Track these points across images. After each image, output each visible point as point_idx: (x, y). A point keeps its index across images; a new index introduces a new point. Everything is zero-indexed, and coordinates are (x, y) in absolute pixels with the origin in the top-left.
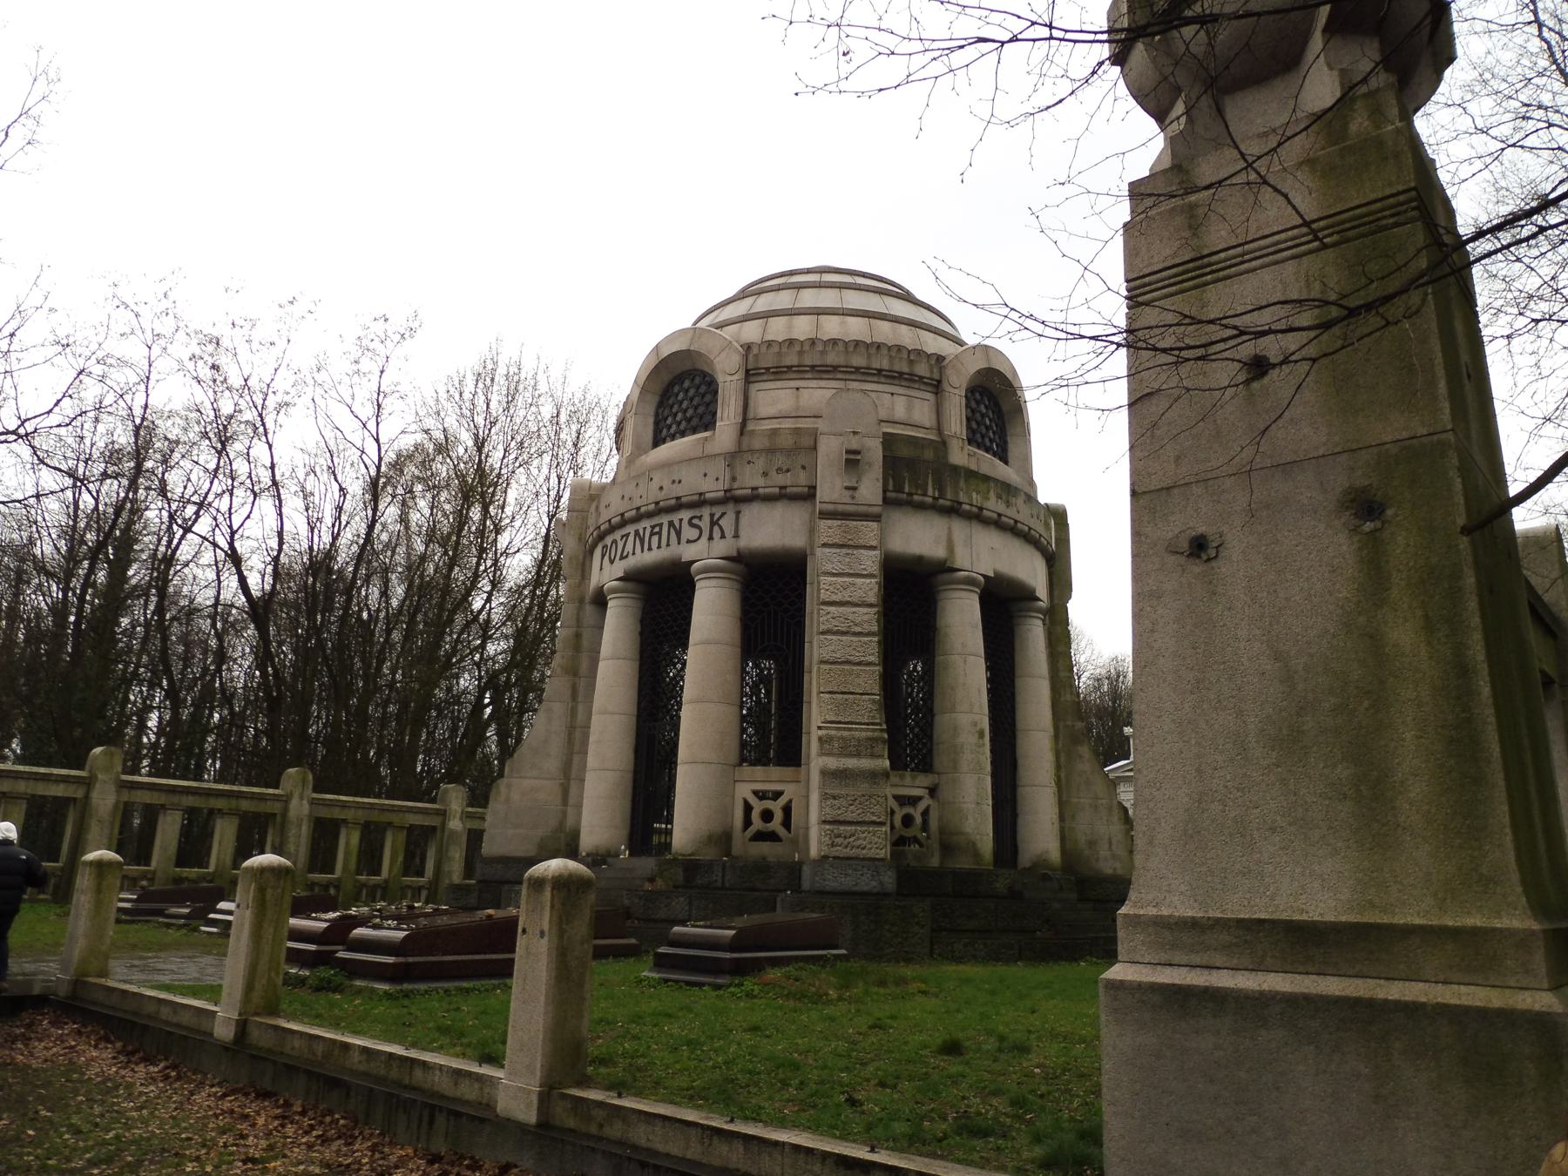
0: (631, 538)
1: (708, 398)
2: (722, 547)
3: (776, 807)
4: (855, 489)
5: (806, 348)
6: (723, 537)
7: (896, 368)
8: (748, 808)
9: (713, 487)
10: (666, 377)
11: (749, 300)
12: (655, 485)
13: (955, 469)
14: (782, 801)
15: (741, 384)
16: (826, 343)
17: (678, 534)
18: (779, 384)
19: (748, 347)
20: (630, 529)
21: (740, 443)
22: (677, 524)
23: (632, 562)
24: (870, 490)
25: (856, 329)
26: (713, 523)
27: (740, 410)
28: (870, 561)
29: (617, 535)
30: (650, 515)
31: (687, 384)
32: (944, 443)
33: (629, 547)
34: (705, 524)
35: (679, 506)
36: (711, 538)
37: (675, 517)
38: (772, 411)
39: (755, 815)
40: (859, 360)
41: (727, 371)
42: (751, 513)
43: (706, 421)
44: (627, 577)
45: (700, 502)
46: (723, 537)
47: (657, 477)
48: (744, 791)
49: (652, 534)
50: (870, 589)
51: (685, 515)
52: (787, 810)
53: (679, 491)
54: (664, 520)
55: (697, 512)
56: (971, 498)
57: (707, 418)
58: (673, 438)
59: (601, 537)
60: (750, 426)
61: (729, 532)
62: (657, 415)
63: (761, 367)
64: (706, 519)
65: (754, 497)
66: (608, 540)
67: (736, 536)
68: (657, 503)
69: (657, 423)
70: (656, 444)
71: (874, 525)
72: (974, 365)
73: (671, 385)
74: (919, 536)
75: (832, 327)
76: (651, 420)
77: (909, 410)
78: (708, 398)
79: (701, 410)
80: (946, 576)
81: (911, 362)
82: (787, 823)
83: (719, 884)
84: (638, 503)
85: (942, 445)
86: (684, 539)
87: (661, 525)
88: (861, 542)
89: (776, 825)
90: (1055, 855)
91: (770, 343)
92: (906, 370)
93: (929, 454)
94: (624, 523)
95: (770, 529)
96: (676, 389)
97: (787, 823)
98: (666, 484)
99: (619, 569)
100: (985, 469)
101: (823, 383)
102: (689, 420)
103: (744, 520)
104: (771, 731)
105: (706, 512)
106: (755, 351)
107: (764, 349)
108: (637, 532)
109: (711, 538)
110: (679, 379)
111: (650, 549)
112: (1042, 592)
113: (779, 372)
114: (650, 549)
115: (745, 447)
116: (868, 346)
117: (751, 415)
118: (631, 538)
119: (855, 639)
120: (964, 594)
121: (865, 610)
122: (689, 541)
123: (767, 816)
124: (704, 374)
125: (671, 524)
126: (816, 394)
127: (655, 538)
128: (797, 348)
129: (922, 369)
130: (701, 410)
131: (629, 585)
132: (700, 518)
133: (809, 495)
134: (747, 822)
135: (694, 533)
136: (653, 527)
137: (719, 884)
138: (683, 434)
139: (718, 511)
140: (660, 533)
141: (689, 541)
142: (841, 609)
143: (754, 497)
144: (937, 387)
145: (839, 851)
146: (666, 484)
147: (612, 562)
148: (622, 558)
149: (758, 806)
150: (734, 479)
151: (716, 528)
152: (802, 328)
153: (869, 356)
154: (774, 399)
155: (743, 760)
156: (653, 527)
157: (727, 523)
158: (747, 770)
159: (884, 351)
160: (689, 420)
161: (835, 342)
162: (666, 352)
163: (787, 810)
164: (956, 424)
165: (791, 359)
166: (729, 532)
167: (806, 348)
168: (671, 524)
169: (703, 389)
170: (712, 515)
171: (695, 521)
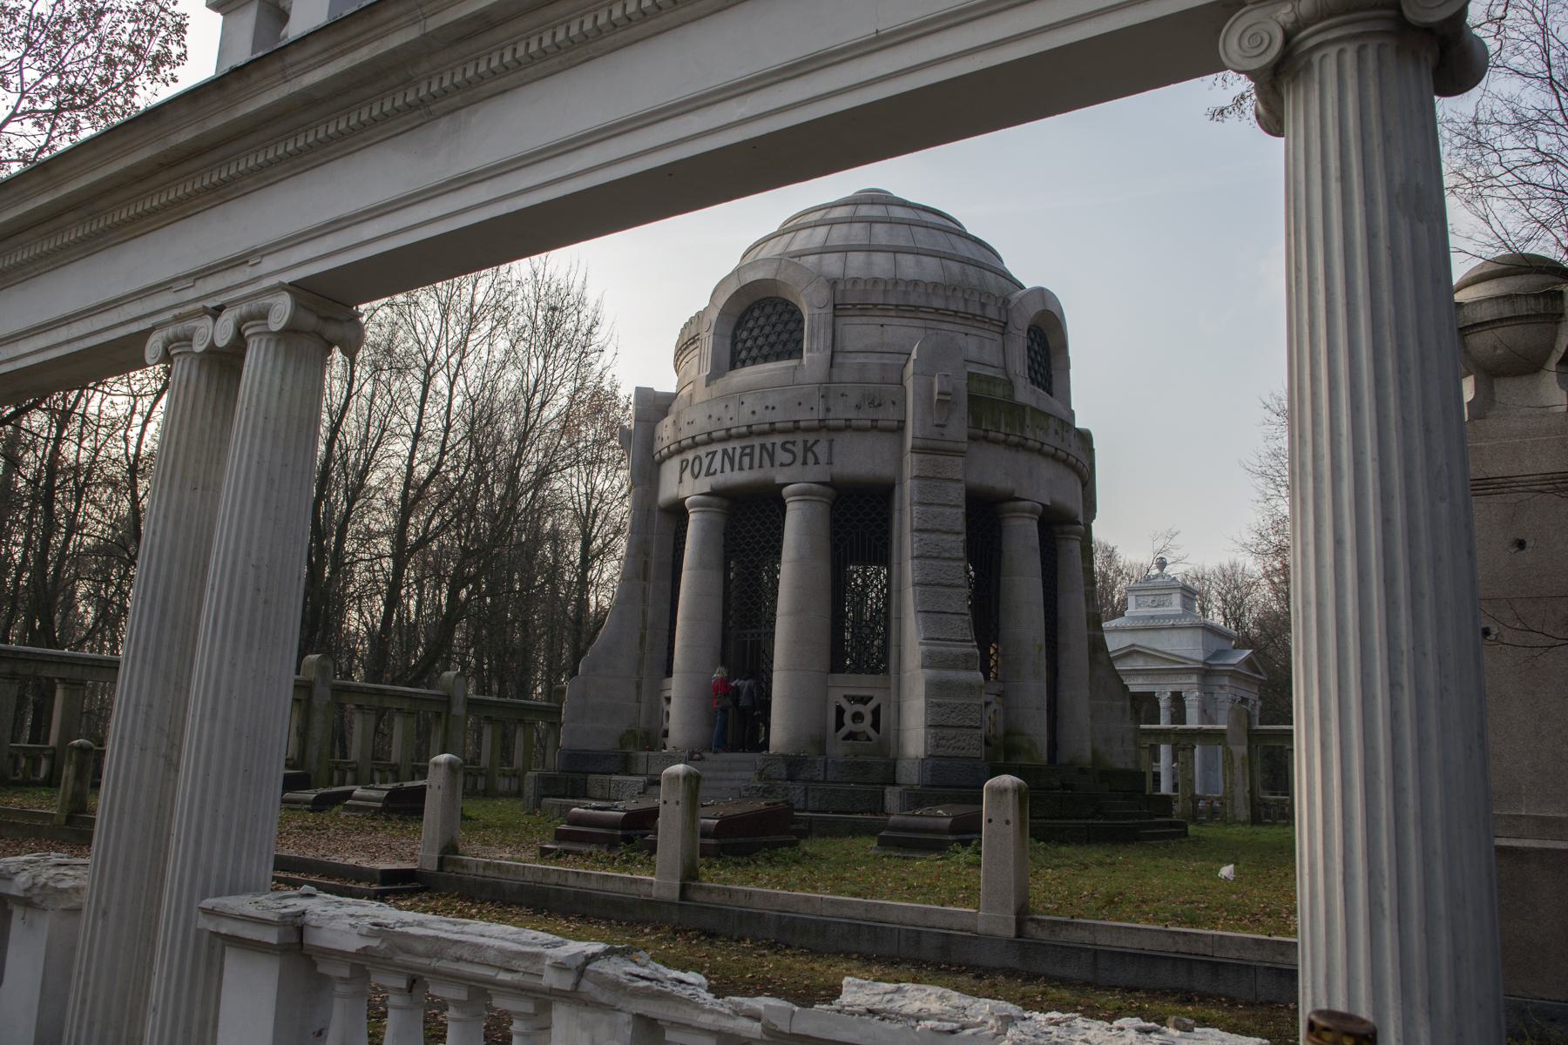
0: (718, 457)
1: (791, 326)
2: (818, 472)
3: (866, 710)
4: (943, 426)
5: (890, 287)
6: (817, 463)
7: (970, 310)
8: (840, 711)
9: (807, 417)
11: (822, 231)
12: (747, 409)
13: (1023, 407)
14: (872, 705)
15: (830, 317)
16: (908, 283)
17: (772, 457)
18: (864, 320)
19: (833, 283)
20: (719, 448)
21: (830, 375)
22: (769, 447)
23: (721, 479)
24: (958, 428)
25: (930, 269)
27: (829, 342)
28: (957, 494)
29: (702, 451)
30: (740, 436)
31: (768, 310)
32: (1011, 382)
33: (717, 464)
34: (799, 449)
35: (773, 430)
36: (805, 463)
37: (768, 441)
38: (860, 346)
39: (847, 718)
40: (938, 303)
41: (811, 306)
42: (841, 440)
43: (790, 348)
44: (714, 493)
45: (796, 428)
46: (817, 463)
47: (748, 400)
48: (837, 696)
50: (956, 517)
51: (778, 440)
52: (876, 712)
53: (771, 416)
54: (757, 442)
55: (790, 438)
56: (1033, 435)
57: (791, 346)
58: (754, 361)
59: (680, 451)
60: (839, 359)
61: (823, 458)
62: (734, 336)
63: (846, 302)
64: (800, 445)
65: (848, 427)
66: (690, 456)
67: (830, 463)
68: (749, 426)
69: (734, 344)
70: (733, 367)
71: (960, 460)
72: (1032, 310)
73: (750, 309)
74: (996, 470)
75: (909, 267)
76: (728, 342)
77: (979, 348)
78: (791, 326)
79: (785, 336)
80: (1012, 504)
81: (983, 306)
82: (876, 725)
83: (821, 778)
84: (728, 424)
85: (1010, 384)
86: (777, 463)
87: (752, 447)
88: (949, 475)
89: (866, 725)
90: (1088, 754)
91: (855, 281)
92: (978, 312)
93: (999, 393)
94: (711, 441)
95: (859, 459)
96: (756, 313)
97: (876, 725)
99: (705, 484)
100: (1043, 407)
101: (905, 321)
102: (772, 346)
103: (837, 448)
104: (856, 643)
105: (799, 438)
106: (841, 287)
107: (849, 286)
108: (725, 452)
109: (805, 463)
110: (761, 304)
112: (1081, 519)
113: (864, 309)
114: (741, 469)
115: (835, 379)
116: (945, 288)
117: (838, 348)
118: (718, 457)
119: (945, 563)
120: (1027, 521)
121: (953, 538)
122: (782, 465)
123: (857, 717)
124: (787, 303)
125: (763, 447)
126: (900, 332)
127: (746, 460)
128: (881, 287)
129: (992, 312)
130: (785, 336)
131: (715, 500)
132: (794, 443)
133: (900, 428)
134: (840, 724)
135: (787, 458)
136: (743, 448)
137: (821, 778)
138: (766, 359)
139: (811, 438)
140: (751, 455)
141: (782, 465)
142: (933, 536)
143: (848, 427)
144: (1004, 328)
145: (941, 751)
146: (759, 408)
148: (708, 474)
149: (850, 710)
150: (828, 410)
151: (810, 455)
152: (881, 265)
153: (947, 298)
154: (859, 333)
155: (836, 666)
156: (743, 448)
157: (821, 450)
158: (839, 678)
159: (959, 294)
160: (772, 346)
161: (916, 283)
162: (750, 277)
163: (876, 712)
164: (1019, 364)
165: (877, 298)
166: (823, 458)
167: (890, 287)
169: (786, 317)
170: (805, 442)
171: (789, 446)
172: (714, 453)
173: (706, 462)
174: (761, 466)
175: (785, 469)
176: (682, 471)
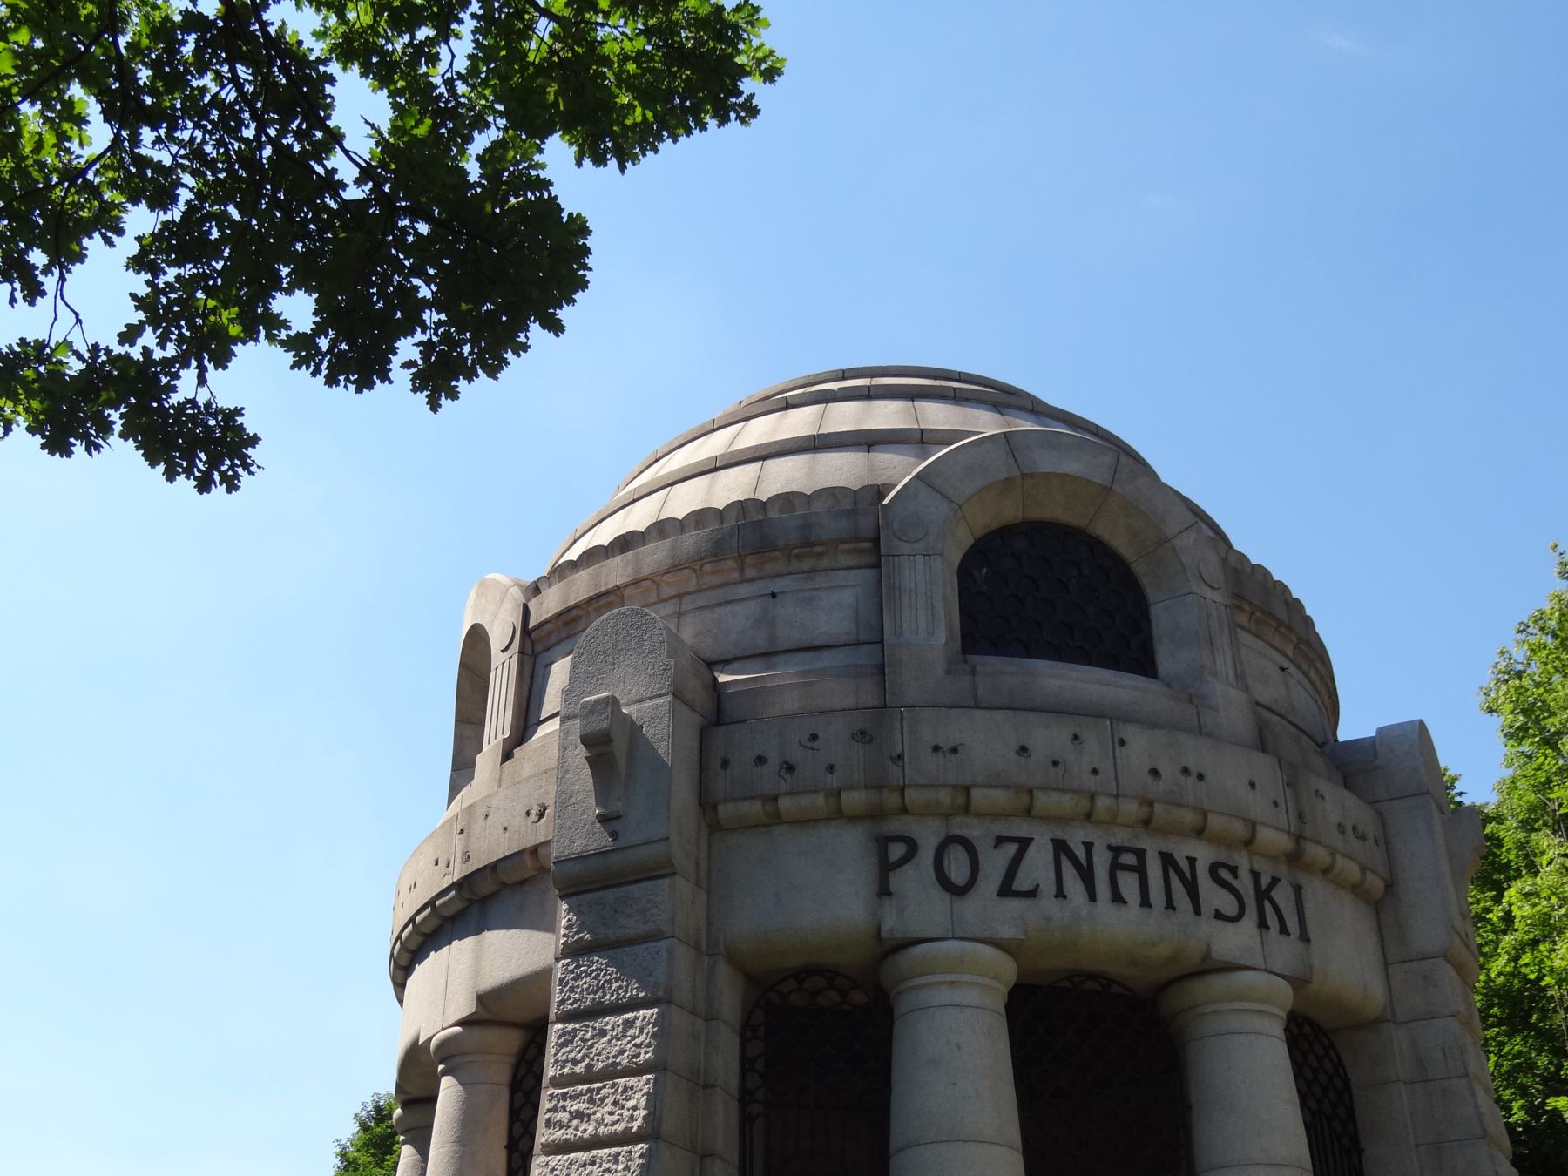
10: (1010, 511)
26: (1263, 895)
34: (1245, 884)
36: (1263, 924)
46: (1284, 930)
49: (1115, 867)
67: (1304, 937)
87: (1140, 854)
98: (1165, 768)
105: (1243, 861)
111: (1117, 898)
114: (1117, 898)
122: (1219, 915)
127: (1129, 884)
140: (1140, 870)
141: (1219, 915)
147: (958, 891)
148: (1006, 890)
156: (1116, 851)
168: (1168, 860)
170: (1256, 876)
172: (1024, 843)
173: (994, 864)
174: (1170, 906)
175: (1230, 926)
176: (886, 868)
